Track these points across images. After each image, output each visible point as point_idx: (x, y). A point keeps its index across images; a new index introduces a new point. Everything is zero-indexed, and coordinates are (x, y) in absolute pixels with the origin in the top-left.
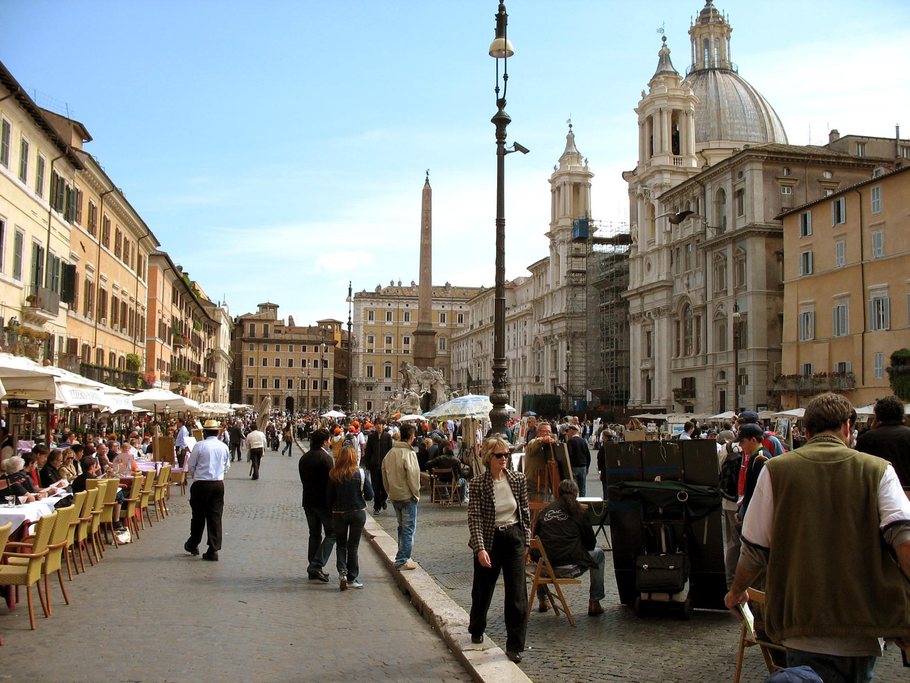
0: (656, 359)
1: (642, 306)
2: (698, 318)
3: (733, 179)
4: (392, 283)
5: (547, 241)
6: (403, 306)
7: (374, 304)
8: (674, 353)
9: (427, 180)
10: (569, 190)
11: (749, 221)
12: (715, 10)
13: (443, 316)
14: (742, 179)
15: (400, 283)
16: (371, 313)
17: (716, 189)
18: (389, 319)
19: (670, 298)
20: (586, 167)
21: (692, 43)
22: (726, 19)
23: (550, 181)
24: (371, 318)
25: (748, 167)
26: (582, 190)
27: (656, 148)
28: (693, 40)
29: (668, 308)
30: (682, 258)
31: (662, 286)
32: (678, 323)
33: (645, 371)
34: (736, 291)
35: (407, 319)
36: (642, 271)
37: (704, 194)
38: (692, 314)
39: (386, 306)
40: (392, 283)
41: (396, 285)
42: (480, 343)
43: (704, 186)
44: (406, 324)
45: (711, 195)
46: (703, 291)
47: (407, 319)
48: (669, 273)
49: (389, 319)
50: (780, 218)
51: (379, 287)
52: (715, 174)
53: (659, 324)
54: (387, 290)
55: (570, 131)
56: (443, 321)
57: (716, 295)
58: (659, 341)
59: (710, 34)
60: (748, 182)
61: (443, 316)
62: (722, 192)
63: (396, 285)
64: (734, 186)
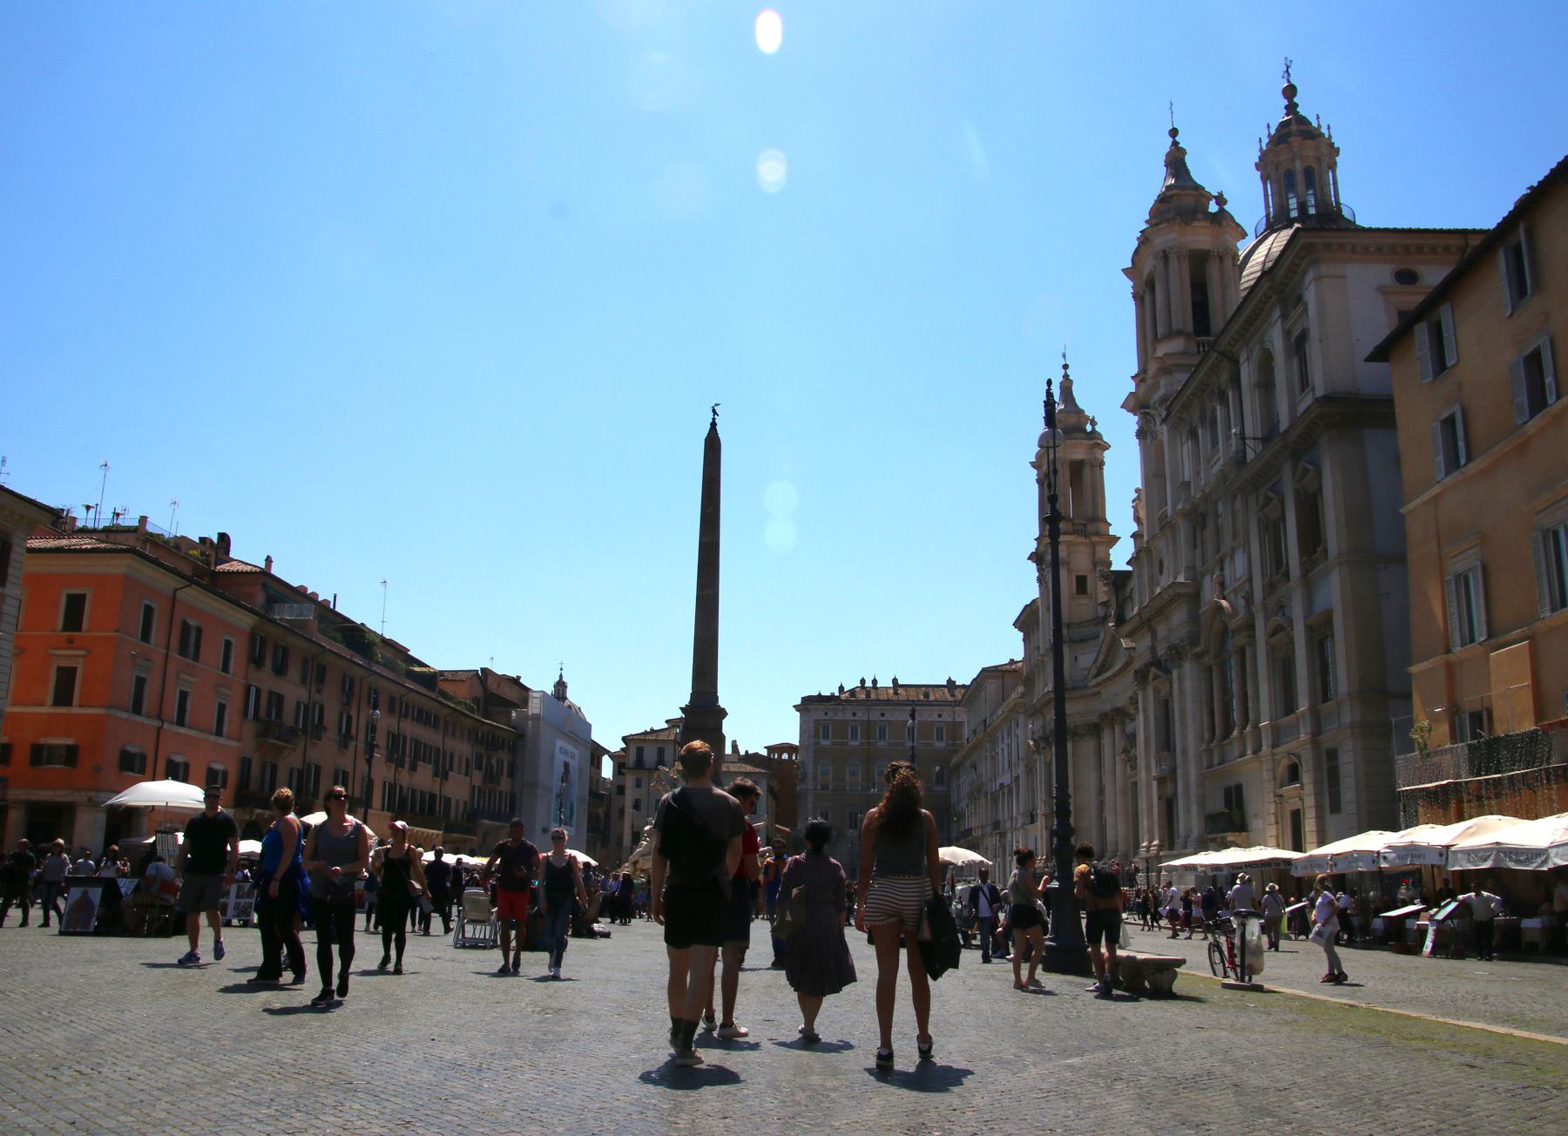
0: (1178, 752)
1: (1153, 649)
2: (1242, 651)
3: (1284, 316)
4: (863, 681)
5: (1033, 566)
6: (875, 716)
7: (831, 714)
8: (1207, 736)
9: (713, 424)
10: (1064, 475)
11: (1320, 393)
12: (1303, 121)
13: (940, 730)
14: (1300, 308)
15: (875, 682)
16: (826, 729)
17: (1256, 353)
18: (854, 737)
19: (1194, 617)
20: (1094, 431)
21: (1265, 184)
22: (1324, 130)
23: (1033, 465)
24: (826, 736)
25: (1310, 275)
26: (1087, 472)
27: (1160, 330)
28: (1264, 179)
29: (1194, 639)
30: (1209, 534)
31: (1179, 596)
32: (1209, 669)
33: (1161, 781)
34: (1307, 568)
35: (882, 737)
36: (1151, 579)
37: (1236, 380)
38: (1233, 643)
39: (849, 716)
40: (863, 681)
41: (869, 684)
42: (974, 767)
43: (1235, 363)
44: (882, 743)
45: (1247, 374)
46: (1247, 587)
47: (882, 737)
48: (1191, 569)
49: (854, 737)
50: (1382, 353)
51: (841, 688)
52: (1250, 322)
53: (1180, 678)
54: (852, 692)
55: (1066, 376)
56: (940, 738)
57: (1270, 588)
58: (1183, 715)
59: (1293, 160)
60: (1312, 308)
61: (940, 730)
62: (1267, 361)
63: (869, 684)
64: (1287, 333)
